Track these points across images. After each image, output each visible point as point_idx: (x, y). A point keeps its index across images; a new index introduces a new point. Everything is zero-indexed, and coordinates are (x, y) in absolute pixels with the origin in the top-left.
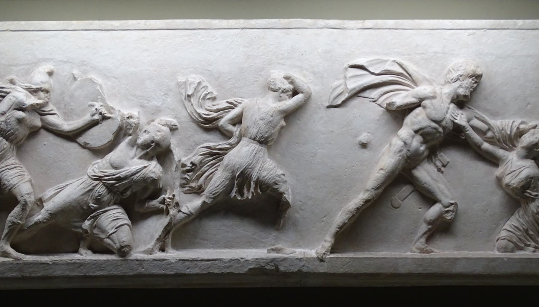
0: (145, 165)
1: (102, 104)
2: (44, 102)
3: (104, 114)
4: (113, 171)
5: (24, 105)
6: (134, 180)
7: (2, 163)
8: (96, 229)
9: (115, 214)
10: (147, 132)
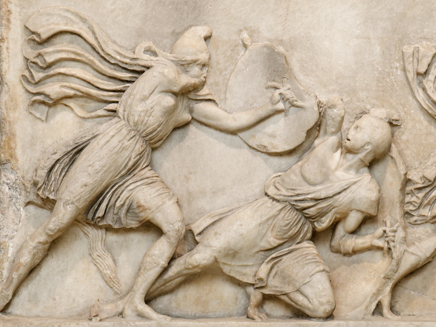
1: (289, 86)
2: (199, 82)
3: (293, 102)
4: (305, 188)
5: (176, 86)
7: (134, 175)
8: (277, 279)
9: (307, 255)
10: (359, 129)
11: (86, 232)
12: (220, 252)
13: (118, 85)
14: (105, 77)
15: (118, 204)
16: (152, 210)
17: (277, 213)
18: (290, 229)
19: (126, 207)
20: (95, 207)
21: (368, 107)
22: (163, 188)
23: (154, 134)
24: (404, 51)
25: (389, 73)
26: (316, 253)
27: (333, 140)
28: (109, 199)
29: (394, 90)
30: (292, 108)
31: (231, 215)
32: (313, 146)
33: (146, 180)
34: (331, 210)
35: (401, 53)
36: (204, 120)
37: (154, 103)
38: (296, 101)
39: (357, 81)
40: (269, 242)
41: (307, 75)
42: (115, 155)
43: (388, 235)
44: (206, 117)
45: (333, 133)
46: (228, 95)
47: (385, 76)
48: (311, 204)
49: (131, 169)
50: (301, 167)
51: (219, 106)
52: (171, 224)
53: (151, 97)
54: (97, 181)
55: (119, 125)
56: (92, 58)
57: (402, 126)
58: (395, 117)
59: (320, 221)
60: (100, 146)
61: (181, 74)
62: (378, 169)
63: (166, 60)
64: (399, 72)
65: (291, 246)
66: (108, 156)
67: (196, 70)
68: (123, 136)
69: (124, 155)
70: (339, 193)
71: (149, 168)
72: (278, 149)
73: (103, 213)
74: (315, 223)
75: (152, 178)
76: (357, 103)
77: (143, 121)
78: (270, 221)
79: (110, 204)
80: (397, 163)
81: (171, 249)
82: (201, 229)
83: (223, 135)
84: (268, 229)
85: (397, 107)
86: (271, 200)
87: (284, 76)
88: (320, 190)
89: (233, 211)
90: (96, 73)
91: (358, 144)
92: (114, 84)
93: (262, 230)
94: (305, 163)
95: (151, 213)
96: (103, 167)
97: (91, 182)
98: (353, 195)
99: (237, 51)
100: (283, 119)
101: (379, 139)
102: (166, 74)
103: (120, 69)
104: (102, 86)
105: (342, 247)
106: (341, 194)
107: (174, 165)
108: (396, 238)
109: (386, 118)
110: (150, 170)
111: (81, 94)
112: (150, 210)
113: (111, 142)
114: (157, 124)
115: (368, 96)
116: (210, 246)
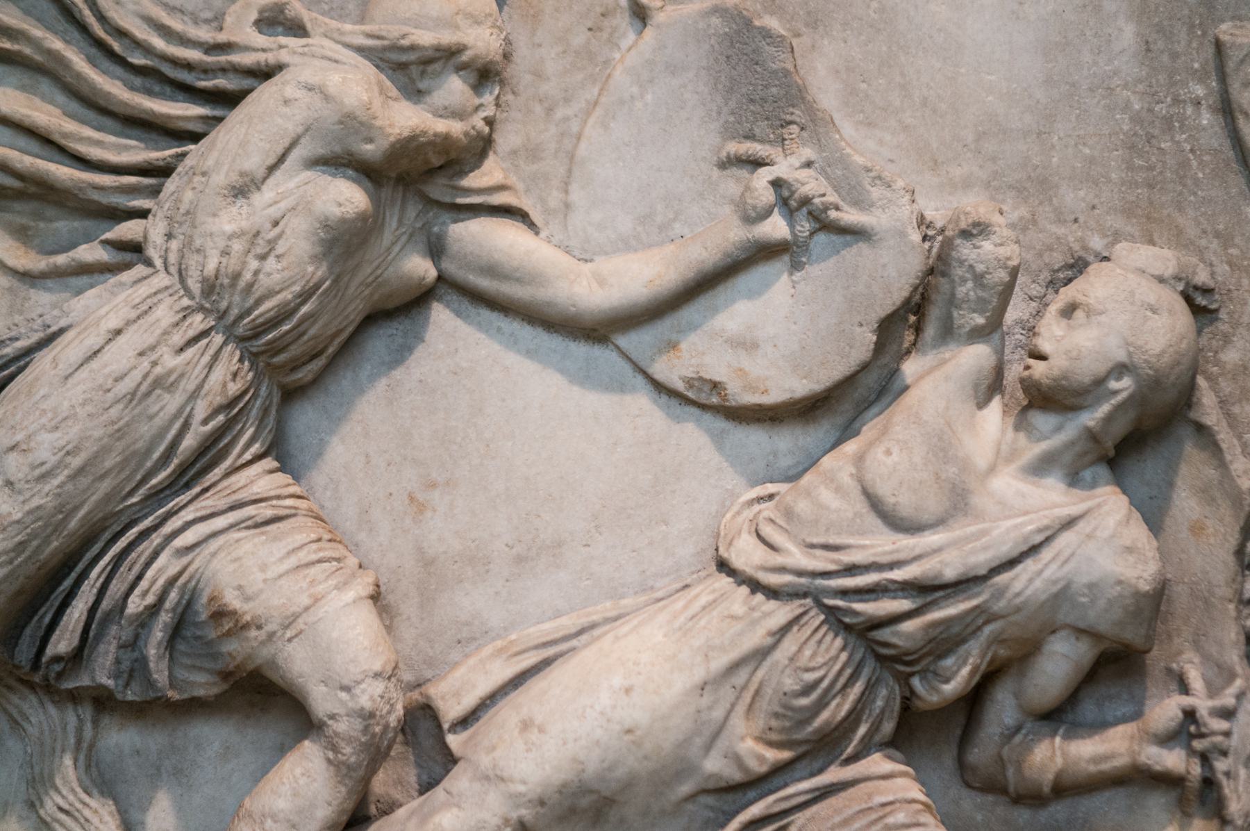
0: (1074, 510)
1: (808, 153)
2: (466, 134)
3: (826, 208)
6: (1009, 594)
7: (206, 490)
9: (888, 809)
10: (1079, 314)
11: (16, 715)
12: (542, 803)
13: (157, 149)
14: (108, 122)
15: (135, 605)
16: (270, 627)
17: (769, 641)
18: (821, 704)
19: (165, 618)
20: (42, 617)
21: (1097, 243)
22: (319, 540)
23: (286, 327)
24: (1225, 38)
25: (1168, 122)
26: (922, 797)
27: (976, 356)
28: (98, 584)
29: (1189, 182)
30: (822, 238)
31: (586, 646)
32: (896, 386)
33: (250, 511)
34: (979, 628)
35: (1210, 51)
36: (484, 283)
37: (283, 205)
38: (837, 208)
39: (1053, 146)
40: (738, 760)
41: (871, 125)
42: (120, 406)
43: (1203, 730)
44: (492, 270)
45: (977, 335)
46: (576, 195)
47: (1156, 132)
48: (903, 605)
49: (193, 464)
50: (859, 459)
51: (543, 234)
52: (346, 689)
53: (271, 181)
54: (40, 513)
55: (144, 290)
56: (57, 44)
57: (1223, 315)
58: (1202, 277)
59: (936, 674)
60: (63, 368)
61: (396, 99)
62: (1148, 467)
63: (339, 47)
64: (1206, 118)
65: (821, 771)
66: (90, 408)
67: (454, 88)
68: (158, 332)
69: (162, 409)
70: (1011, 563)
71: (268, 463)
72: (765, 392)
73: (76, 642)
74: (916, 682)
75: (274, 502)
76: (1054, 229)
77: (236, 276)
78: (741, 677)
79: (105, 604)
80: (1224, 446)
81: (343, 789)
82: (469, 701)
83: (554, 342)
84: (733, 706)
85: (1203, 242)
86: (744, 590)
87: (789, 118)
88: (937, 550)
89: (596, 632)
90: (74, 106)
91: (1087, 369)
92: (142, 145)
93: (710, 708)
94: (871, 444)
95: (263, 643)
96: (68, 453)
97: (18, 516)
98: (1066, 569)
99: (611, 34)
100: (785, 277)
101: (1163, 352)
102: (332, 90)
103: (168, 89)
104: (95, 153)
105: (1010, 772)
106: (1019, 568)
107: (367, 456)
108: (1234, 741)
109: (1178, 278)
110: (271, 472)
111: (16, 184)
112: (259, 627)
113: (105, 356)
114: (297, 288)
115: (1096, 201)
116: (502, 779)
